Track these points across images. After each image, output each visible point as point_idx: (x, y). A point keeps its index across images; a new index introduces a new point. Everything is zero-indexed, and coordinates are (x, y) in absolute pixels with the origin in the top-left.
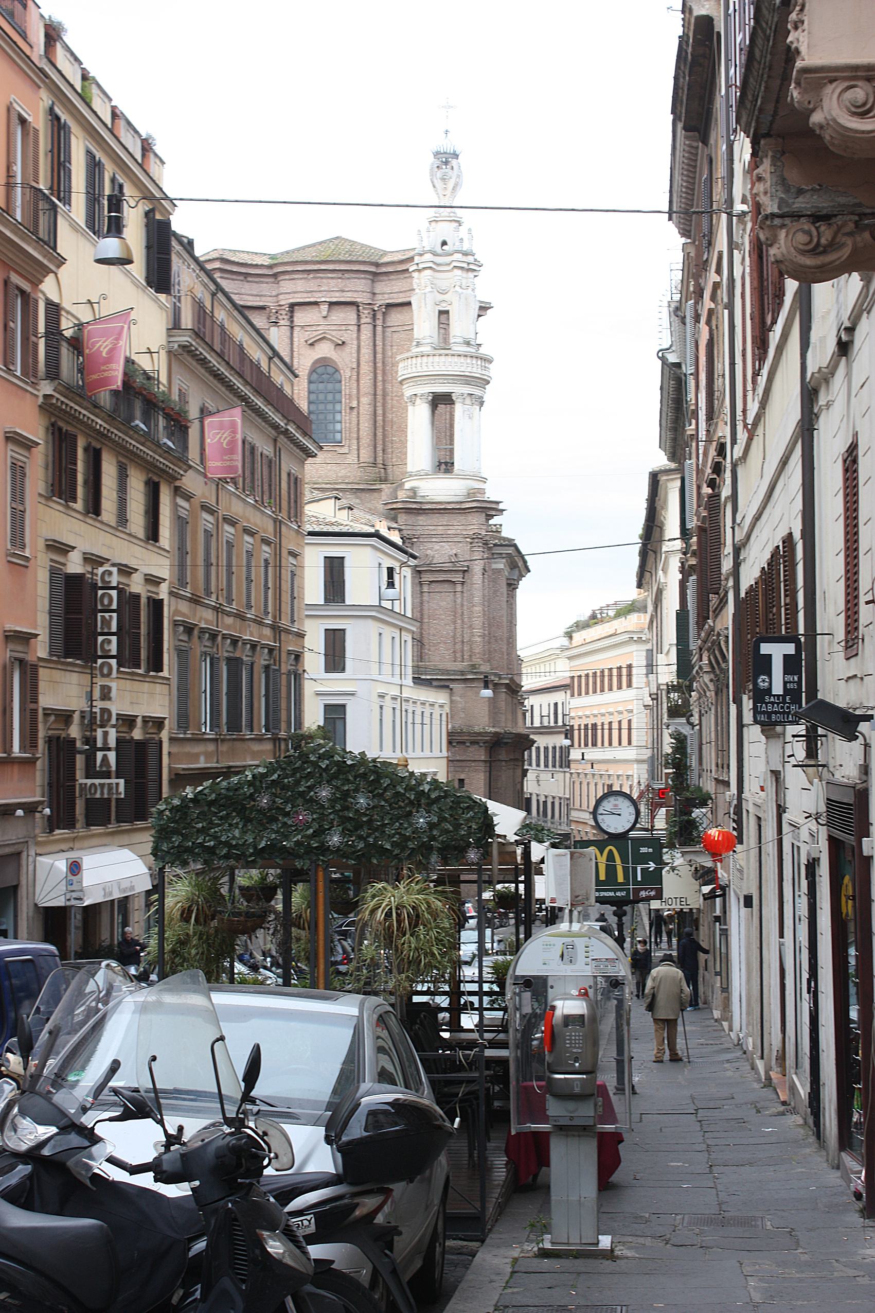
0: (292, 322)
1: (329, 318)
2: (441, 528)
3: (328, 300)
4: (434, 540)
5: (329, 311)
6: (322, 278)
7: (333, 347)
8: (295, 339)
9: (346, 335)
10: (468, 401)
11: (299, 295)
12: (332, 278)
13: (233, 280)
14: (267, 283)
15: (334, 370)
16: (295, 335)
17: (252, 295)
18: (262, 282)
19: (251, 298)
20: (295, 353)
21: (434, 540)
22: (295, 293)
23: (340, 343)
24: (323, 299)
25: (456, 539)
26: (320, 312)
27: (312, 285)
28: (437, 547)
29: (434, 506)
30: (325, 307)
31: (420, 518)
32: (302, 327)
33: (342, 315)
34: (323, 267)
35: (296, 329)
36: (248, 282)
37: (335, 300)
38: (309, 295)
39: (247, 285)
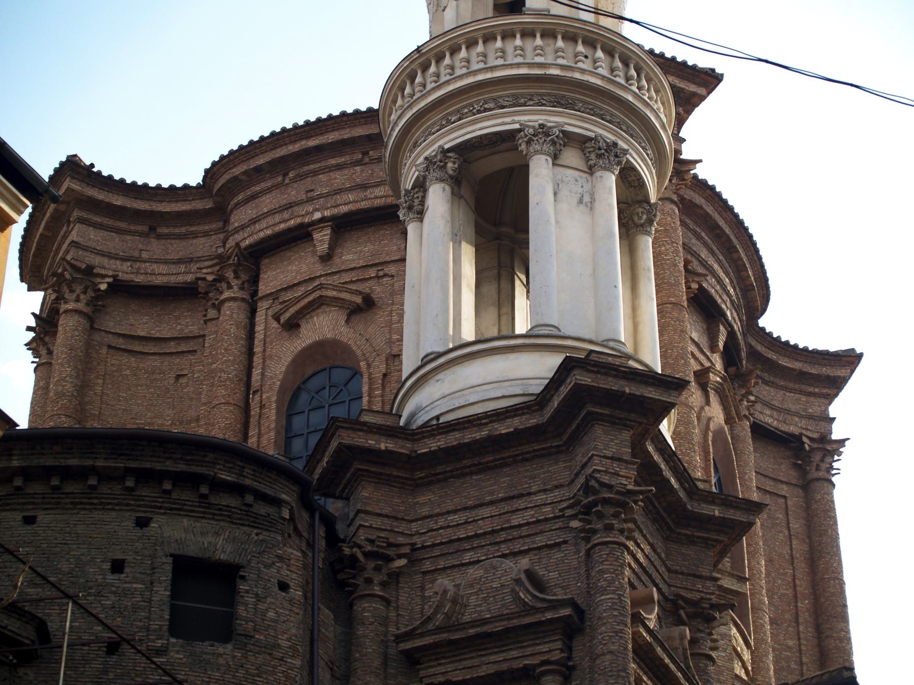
0: (255, 293)
1: (336, 260)
2: (486, 512)
3: (327, 213)
4: (467, 557)
5: (332, 247)
6: (315, 173)
7: (342, 318)
8: (259, 328)
9: (378, 289)
10: (571, 156)
11: (263, 224)
12: (339, 167)
13: (118, 231)
14: (206, 234)
15: (349, 373)
16: (260, 317)
17: (166, 262)
18: (195, 235)
19: (163, 269)
20: (257, 360)
21: (467, 557)
22: (254, 221)
23: (358, 300)
24: (317, 215)
25: (540, 541)
26: (314, 252)
27: (294, 193)
28: (474, 573)
29: (453, 439)
30: (322, 238)
31: (422, 499)
32: (274, 296)
33: (368, 248)
34: (312, 143)
35: (263, 306)
36: (159, 237)
37: (344, 209)
38: (286, 215)
39: (156, 248)
